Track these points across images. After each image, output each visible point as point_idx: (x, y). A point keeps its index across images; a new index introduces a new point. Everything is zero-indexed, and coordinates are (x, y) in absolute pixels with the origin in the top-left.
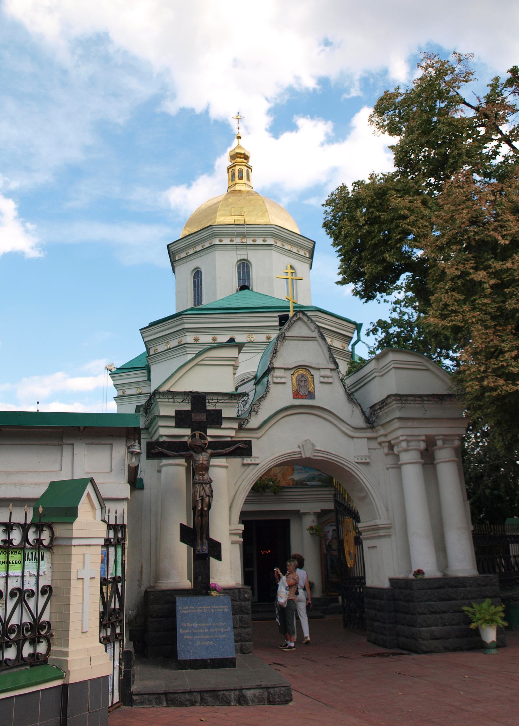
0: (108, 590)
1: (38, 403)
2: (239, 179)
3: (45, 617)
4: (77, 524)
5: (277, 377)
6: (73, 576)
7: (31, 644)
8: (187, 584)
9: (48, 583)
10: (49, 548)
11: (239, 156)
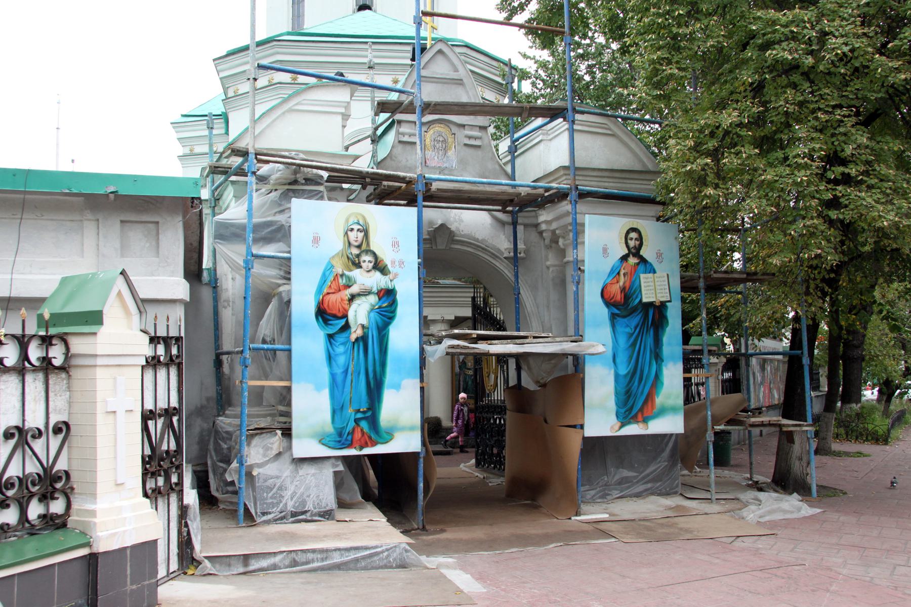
0: (156, 426)
1: (73, 161)
7: (40, 500)
9: (65, 418)
10: (63, 368)
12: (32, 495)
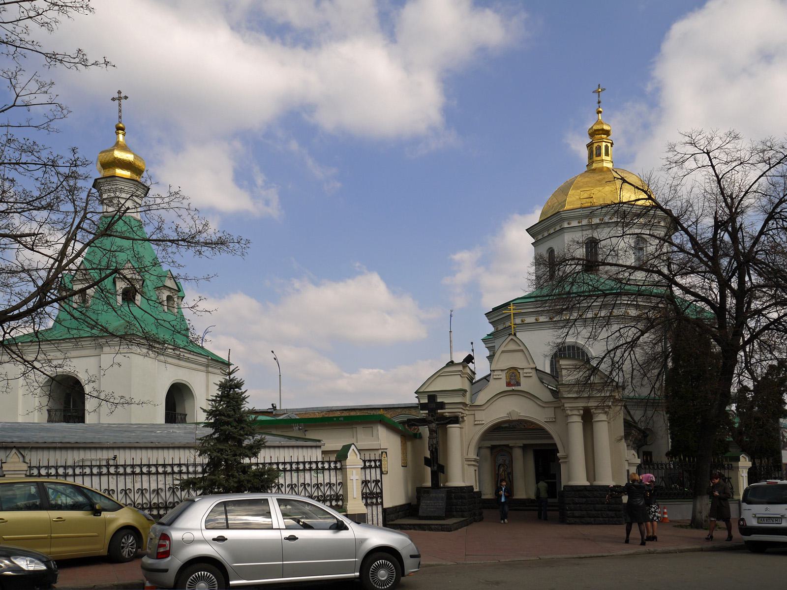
2: (596, 156)
3: (341, 492)
4: (348, 460)
5: (496, 375)
6: (348, 479)
8: (428, 483)
11: (597, 133)
12: (333, 499)
